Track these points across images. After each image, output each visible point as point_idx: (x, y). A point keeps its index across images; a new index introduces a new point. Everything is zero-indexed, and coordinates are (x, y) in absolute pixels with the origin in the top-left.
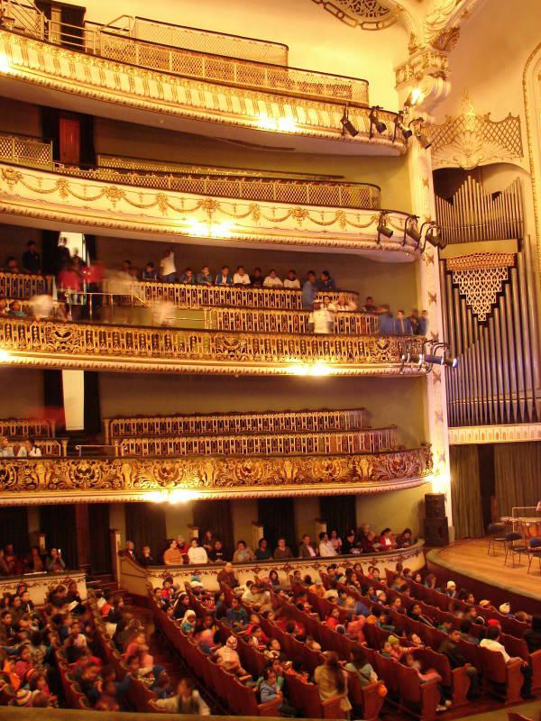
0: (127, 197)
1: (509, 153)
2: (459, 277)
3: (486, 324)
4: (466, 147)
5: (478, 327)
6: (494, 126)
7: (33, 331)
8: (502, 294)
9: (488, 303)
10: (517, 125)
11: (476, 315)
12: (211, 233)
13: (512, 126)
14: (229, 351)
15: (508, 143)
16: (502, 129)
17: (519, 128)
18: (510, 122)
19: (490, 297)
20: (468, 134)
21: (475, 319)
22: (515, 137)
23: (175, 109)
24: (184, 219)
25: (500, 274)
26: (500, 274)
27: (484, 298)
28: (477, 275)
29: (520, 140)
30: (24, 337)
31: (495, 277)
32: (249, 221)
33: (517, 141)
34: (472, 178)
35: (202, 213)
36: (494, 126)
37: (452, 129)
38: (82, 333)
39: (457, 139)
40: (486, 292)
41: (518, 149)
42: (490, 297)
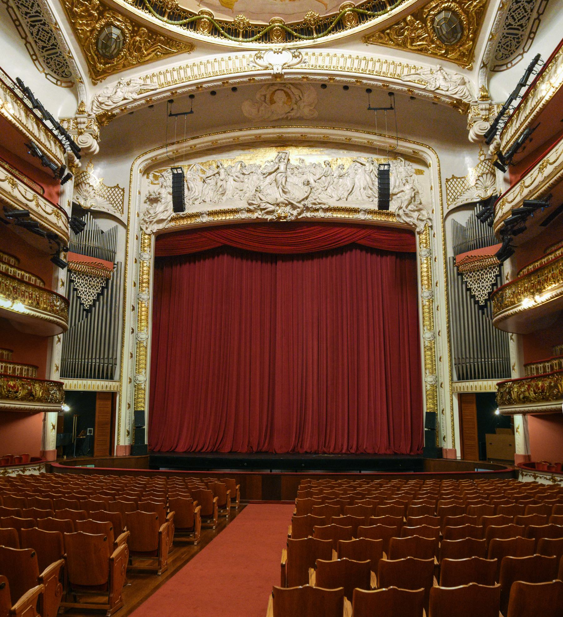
1: (113, 208)
2: (75, 276)
3: (89, 311)
4: (85, 193)
5: (83, 313)
6: (105, 188)
8: (102, 293)
9: (91, 298)
10: (122, 193)
11: (83, 304)
13: (118, 192)
15: (113, 202)
16: (114, 192)
17: (123, 195)
18: (117, 190)
19: (93, 294)
20: (88, 186)
21: (82, 306)
22: (119, 200)
25: (102, 281)
26: (102, 281)
27: (89, 294)
28: (87, 278)
29: (123, 203)
31: (98, 282)
33: (121, 203)
34: (90, 215)
36: (109, 189)
37: (79, 178)
39: (80, 185)
40: (91, 290)
41: (120, 208)
42: (93, 294)
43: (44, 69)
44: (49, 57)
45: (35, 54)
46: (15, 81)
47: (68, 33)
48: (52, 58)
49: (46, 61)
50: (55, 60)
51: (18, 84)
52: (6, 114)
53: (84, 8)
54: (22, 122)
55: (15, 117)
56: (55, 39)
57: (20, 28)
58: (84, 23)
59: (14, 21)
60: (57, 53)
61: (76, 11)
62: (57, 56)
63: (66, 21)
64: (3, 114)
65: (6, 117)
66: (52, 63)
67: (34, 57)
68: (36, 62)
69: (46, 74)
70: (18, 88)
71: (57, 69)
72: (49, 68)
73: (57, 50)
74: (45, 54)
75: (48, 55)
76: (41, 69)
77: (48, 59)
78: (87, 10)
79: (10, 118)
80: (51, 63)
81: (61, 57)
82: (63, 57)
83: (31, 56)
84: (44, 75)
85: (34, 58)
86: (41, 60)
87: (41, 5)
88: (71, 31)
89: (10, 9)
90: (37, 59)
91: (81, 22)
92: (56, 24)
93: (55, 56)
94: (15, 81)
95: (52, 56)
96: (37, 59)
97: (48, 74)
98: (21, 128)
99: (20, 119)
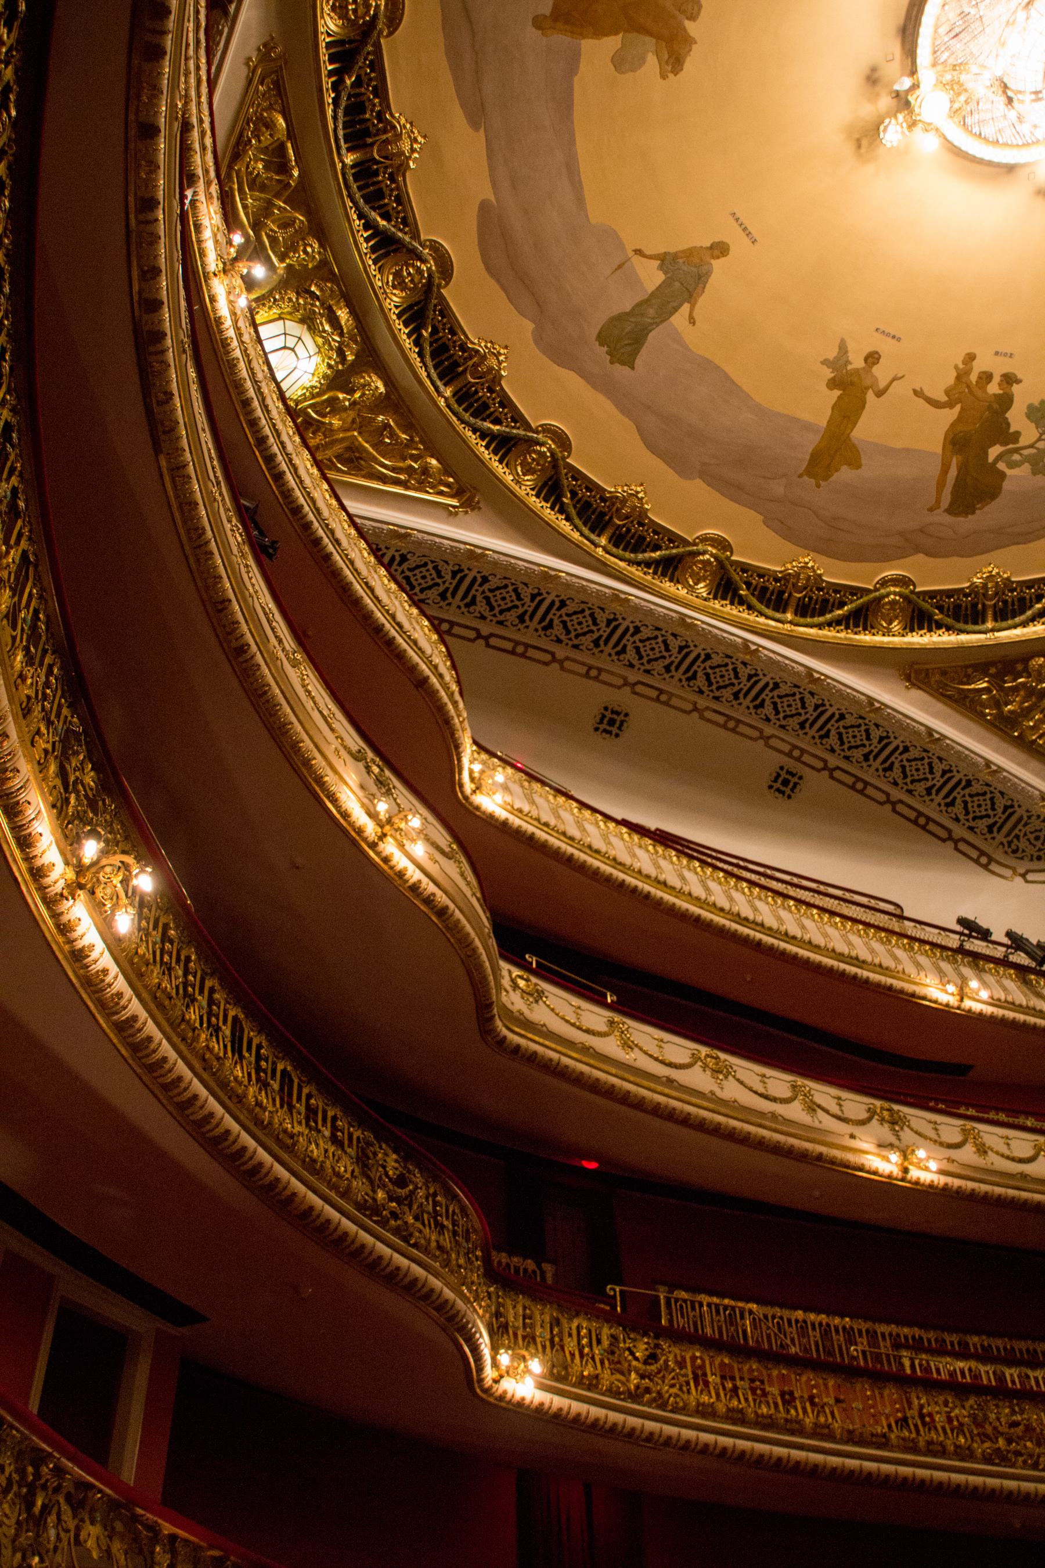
0: (738, 1076)
7: (579, 1338)
12: (906, 1170)
14: (1009, 1441)
23: (783, 945)
24: (852, 1136)
30: (562, 1348)
32: (968, 1154)
35: (879, 1130)
38: (684, 1358)
43: (1014, 870)
44: (1010, 839)
45: (982, 853)
46: (958, 928)
47: (1019, 764)
48: (1017, 837)
49: (1009, 850)
50: (1025, 834)
51: (966, 932)
52: (977, 1007)
53: (1022, 693)
54: (1017, 1003)
55: (995, 1003)
56: (1002, 793)
57: (931, 827)
58: (1038, 720)
59: (915, 822)
60: (1021, 818)
61: (1010, 711)
62: (1025, 825)
63: (1004, 745)
64: (969, 1011)
65: (981, 1014)
66: (1023, 844)
67: (984, 860)
68: (993, 867)
69: (1023, 876)
70: (970, 936)
71: (1040, 850)
72: (1022, 858)
73: (1020, 812)
74: (1000, 837)
75: (1008, 835)
76: (1008, 873)
77: (1010, 843)
78: (1031, 692)
79: (988, 1010)
80: (1021, 846)
81: (1033, 818)
82: (1039, 817)
83: (977, 861)
84: (1019, 880)
85: (984, 861)
86: (999, 855)
87: (943, 755)
88: (1023, 756)
89: (900, 807)
90: (991, 860)
91: (1031, 724)
92: (988, 763)
93: (1020, 827)
94: (958, 928)
95: (1016, 831)
96: (991, 860)
97: (1027, 872)
98: (1021, 1017)
99: (1010, 999)
